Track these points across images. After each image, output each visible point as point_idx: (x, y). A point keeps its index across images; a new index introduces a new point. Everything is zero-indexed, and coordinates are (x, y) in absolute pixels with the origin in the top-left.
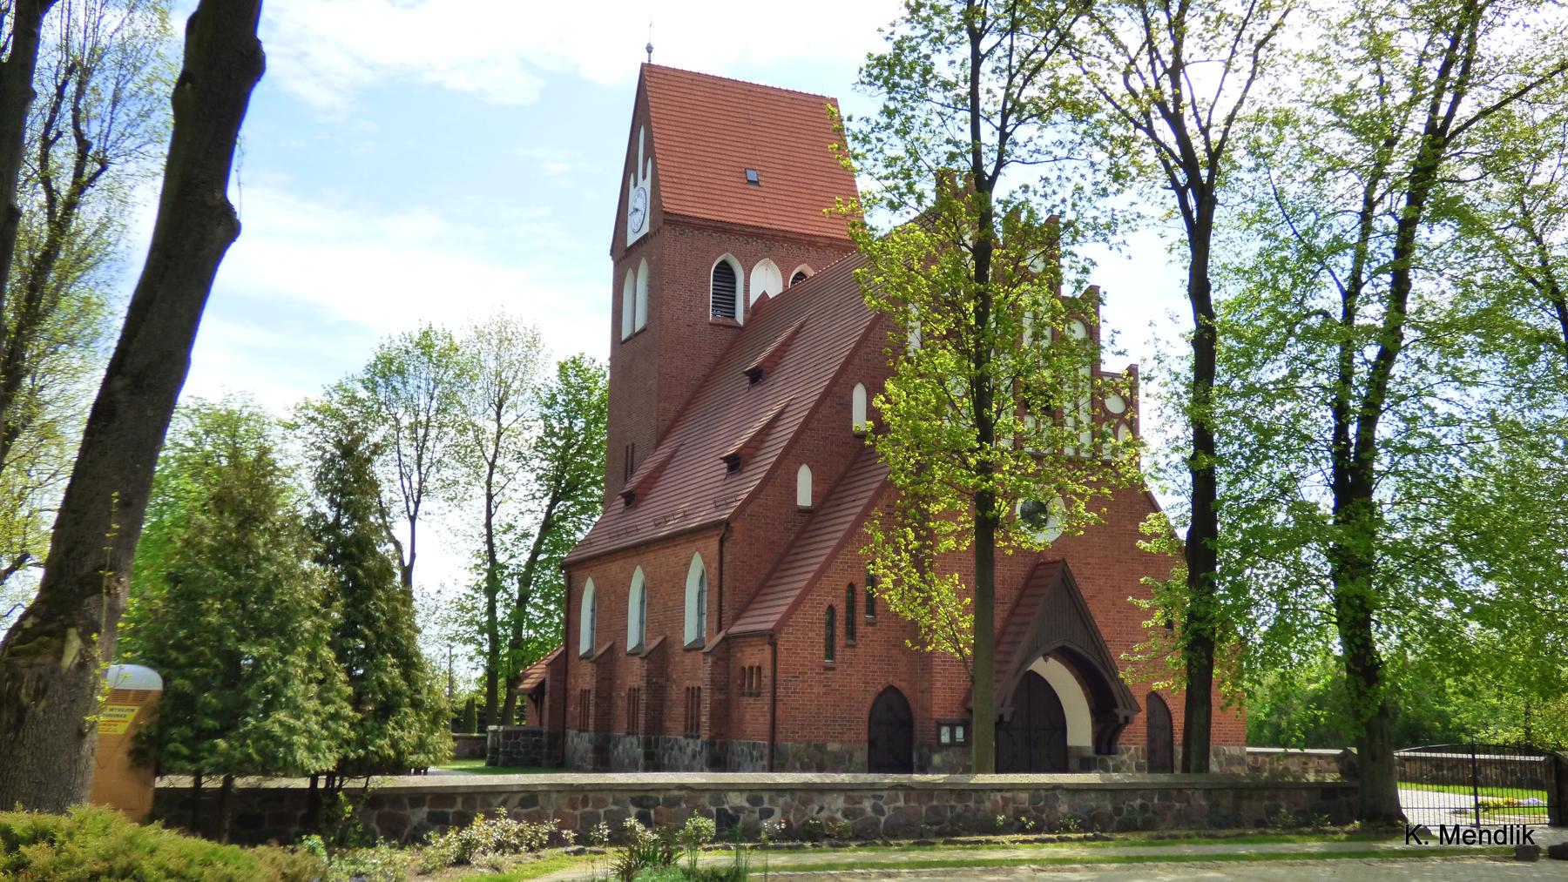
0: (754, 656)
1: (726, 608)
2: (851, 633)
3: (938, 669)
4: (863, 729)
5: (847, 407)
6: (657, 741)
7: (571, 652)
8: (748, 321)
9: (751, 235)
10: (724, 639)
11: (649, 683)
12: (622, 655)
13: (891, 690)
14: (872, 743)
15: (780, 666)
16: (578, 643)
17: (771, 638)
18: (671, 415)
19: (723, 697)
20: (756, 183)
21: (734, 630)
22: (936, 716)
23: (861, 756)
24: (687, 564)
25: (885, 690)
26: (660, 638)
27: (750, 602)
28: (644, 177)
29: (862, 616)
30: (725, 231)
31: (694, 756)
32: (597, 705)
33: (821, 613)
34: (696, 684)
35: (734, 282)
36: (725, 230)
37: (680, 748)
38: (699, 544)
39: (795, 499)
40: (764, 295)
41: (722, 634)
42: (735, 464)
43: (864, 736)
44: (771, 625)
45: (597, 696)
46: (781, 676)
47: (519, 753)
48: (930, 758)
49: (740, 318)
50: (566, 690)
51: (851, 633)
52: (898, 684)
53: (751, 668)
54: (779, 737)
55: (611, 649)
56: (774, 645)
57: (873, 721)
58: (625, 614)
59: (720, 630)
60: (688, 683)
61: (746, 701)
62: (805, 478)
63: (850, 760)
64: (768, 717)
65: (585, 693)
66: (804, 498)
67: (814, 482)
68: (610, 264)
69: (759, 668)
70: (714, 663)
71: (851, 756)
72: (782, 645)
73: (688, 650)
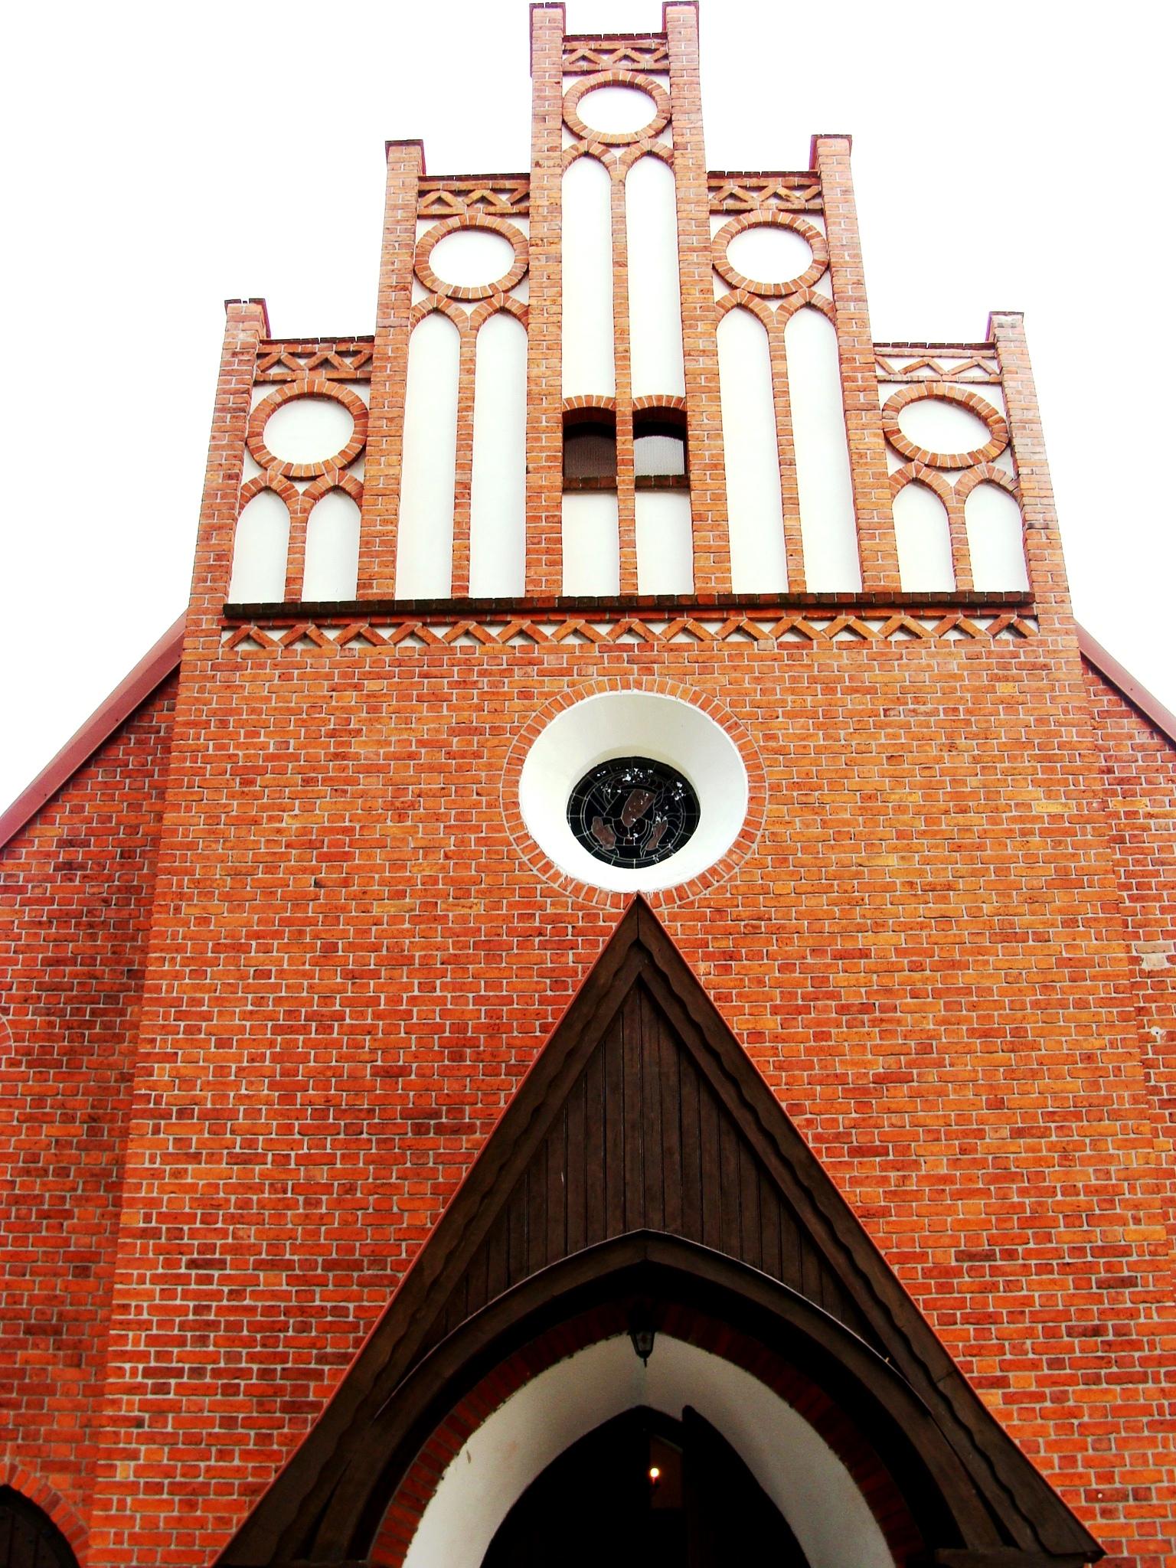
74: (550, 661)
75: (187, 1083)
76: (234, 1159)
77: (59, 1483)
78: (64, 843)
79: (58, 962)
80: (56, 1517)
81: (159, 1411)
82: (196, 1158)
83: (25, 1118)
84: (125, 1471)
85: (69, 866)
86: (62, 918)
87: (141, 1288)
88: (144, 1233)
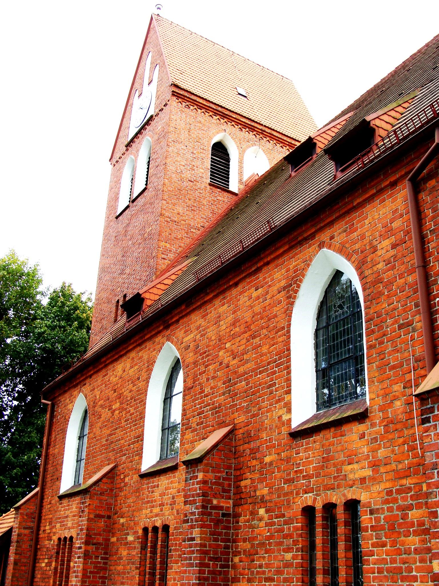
9: (245, 126)
11: (206, 507)
12: (132, 480)
16: (59, 479)
20: (245, 97)
24: (291, 290)
26: (224, 431)
30: (224, 116)
32: (86, 556)
34: (338, 497)
35: (228, 160)
38: (324, 236)
45: (87, 543)
50: (37, 540)
55: (111, 475)
60: (308, 499)
65: (66, 543)
73: (301, 434)
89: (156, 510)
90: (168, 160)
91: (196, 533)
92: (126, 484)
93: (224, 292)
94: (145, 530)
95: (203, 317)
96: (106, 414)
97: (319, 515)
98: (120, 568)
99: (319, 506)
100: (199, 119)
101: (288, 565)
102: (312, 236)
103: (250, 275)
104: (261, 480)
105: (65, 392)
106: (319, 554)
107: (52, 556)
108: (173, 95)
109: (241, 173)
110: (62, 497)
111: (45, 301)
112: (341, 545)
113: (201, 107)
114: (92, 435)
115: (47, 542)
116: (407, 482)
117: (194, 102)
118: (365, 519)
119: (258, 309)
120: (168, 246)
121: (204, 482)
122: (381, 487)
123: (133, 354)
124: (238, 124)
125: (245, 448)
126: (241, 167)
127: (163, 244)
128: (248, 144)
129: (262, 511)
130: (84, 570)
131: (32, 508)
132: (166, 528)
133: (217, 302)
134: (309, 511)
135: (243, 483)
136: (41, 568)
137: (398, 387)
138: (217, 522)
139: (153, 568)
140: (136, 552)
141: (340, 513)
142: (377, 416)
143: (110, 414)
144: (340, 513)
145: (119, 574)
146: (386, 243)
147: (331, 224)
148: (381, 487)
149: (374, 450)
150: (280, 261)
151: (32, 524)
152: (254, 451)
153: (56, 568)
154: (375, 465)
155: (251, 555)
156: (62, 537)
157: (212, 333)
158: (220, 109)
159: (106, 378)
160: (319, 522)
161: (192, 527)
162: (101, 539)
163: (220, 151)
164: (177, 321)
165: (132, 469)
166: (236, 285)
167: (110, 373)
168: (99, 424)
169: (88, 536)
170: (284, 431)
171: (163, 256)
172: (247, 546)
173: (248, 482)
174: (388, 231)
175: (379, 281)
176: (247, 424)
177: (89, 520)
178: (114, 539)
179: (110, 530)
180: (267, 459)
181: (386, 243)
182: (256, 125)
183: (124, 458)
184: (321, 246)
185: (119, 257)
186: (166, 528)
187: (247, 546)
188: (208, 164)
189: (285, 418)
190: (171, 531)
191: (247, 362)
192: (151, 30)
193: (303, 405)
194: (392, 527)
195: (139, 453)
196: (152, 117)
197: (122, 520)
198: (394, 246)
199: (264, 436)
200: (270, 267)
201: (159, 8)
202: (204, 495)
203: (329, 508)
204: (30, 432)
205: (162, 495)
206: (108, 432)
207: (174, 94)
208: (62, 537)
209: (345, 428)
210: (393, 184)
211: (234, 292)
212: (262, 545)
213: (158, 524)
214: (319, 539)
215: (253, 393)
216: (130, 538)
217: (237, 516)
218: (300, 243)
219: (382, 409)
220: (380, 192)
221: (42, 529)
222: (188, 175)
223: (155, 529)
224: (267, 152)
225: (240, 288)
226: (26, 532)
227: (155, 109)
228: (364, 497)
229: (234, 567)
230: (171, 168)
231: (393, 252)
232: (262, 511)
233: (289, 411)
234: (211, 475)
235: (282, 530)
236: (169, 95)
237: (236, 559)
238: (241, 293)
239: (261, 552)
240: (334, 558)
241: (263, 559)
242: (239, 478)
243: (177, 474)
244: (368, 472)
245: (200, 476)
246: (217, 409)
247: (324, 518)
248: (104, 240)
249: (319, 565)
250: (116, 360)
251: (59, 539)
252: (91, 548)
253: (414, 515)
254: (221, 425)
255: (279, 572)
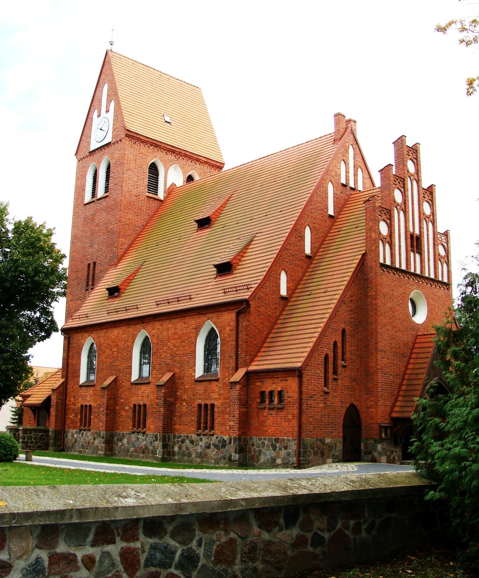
0: (269, 386)
1: (242, 354)
2: (335, 372)
3: (380, 394)
4: (341, 429)
5: (303, 238)
6: (169, 437)
7: (71, 383)
8: (166, 198)
10: (247, 374)
11: (165, 401)
12: (126, 385)
13: (352, 406)
14: (344, 438)
15: (304, 390)
16: (78, 376)
17: (297, 373)
18: (125, 246)
19: (245, 410)
21: (252, 368)
22: (379, 421)
23: (340, 447)
24: (197, 330)
25: (350, 406)
27: (259, 351)
28: (107, 111)
29: (340, 362)
31: (208, 447)
33: (322, 359)
34: (209, 402)
35: (157, 175)
36: (156, 145)
37: (192, 442)
38: (210, 315)
39: (279, 290)
40: (173, 185)
41: (241, 373)
42: (224, 269)
43: (341, 434)
44: (299, 365)
45: (107, 409)
46: (304, 396)
47: (32, 442)
48: (377, 446)
49: (161, 195)
50: (66, 405)
51: (335, 372)
52: (355, 403)
53: (271, 392)
54: (303, 434)
55: (115, 381)
56: (300, 377)
57: (345, 426)
58: (131, 358)
59: (237, 369)
60: (200, 401)
61: (265, 413)
62: (283, 278)
63: (335, 448)
64: (295, 423)
66: (283, 292)
67: (288, 282)
68: (75, 161)
69: (280, 393)
70: (241, 388)
71: (336, 445)
72: (305, 379)
73: (198, 381)
74: (411, 283)
75: (382, 346)
76: (387, 359)
77: (358, 403)
78: (351, 296)
79: (351, 318)
80: (358, 408)
81: (382, 395)
82: (384, 358)
83: (350, 345)
84: (380, 403)
85: (351, 301)
86: (351, 310)
87: (380, 378)
88: (380, 369)
89: (140, 398)
90: (124, 184)
91: (162, 409)
92: (123, 386)
93: (171, 319)
94: (135, 405)
95: (161, 325)
96: (108, 352)
97: (203, 407)
98: (122, 419)
99: (203, 404)
100: (142, 151)
101: (192, 421)
102: (206, 314)
103: (182, 317)
104: (184, 394)
105: (78, 333)
106: (202, 418)
107: (77, 413)
108: (126, 136)
109: (165, 186)
110: (81, 386)
111: (10, 227)
112: (209, 416)
113: (143, 142)
114: (100, 360)
115: (72, 406)
116: (227, 401)
117: (139, 139)
118: (216, 409)
119: (184, 332)
120: (124, 240)
121: (165, 393)
122: (221, 401)
123: (124, 328)
124: (164, 150)
125: (179, 382)
126: (166, 181)
127: (121, 239)
128: (170, 163)
129: (184, 404)
130: (106, 421)
131: (61, 390)
132: (145, 406)
133: (167, 322)
134: (200, 405)
135: (178, 393)
136: (70, 418)
137: (227, 374)
138: (169, 406)
139: (139, 419)
140: (130, 414)
141: (209, 407)
142: (221, 381)
143: (111, 352)
144: (209, 407)
145: (121, 422)
146: (228, 328)
147: (212, 313)
148: (221, 401)
149: (220, 391)
150: (194, 317)
151: (62, 397)
152: (182, 383)
153: (81, 419)
154: (219, 395)
155: (180, 417)
156: (84, 405)
157: (165, 333)
158: (154, 142)
159: (107, 334)
160: (203, 409)
161: (160, 407)
162: (112, 408)
163: (153, 168)
164: (148, 322)
165: (126, 380)
166: (176, 318)
167: (110, 332)
168: (105, 355)
169: (107, 407)
170: (193, 378)
171: (121, 247)
172: (179, 414)
173: (179, 393)
174: (229, 325)
175: (225, 340)
176: (180, 373)
177: (107, 400)
178: (118, 408)
179: (116, 404)
180: (187, 387)
181: (228, 328)
182: (176, 149)
183: (121, 374)
184: (208, 319)
185: (89, 234)
186: (145, 406)
187: (179, 414)
188: (146, 183)
189: (193, 374)
190: (147, 406)
191: (180, 350)
192: (106, 63)
193: (199, 371)
194: (223, 413)
195: (130, 374)
196: (110, 143)
197: (122, 400)
198: (230, 330)
199: (186, 379)
200: (190, 317)
201: (111, 44)
202: (165, 397)
203: (206, 405)
204: (13, 328)
205: (143, 393)
206: (111, 361)
207: (127, 135)
208: (84, 405)
209: (212, 382)
210: (232, 310)
211: (175, 321)
212: (184, 414)
213: (141, 403)
214: (202, 414)
215: (182, 363)
216: (127, 408)
217: (175, 404)
218: (201, 314)
219: (223, 379)
220: (229, 310)
221: (68, 400)
222: (135, 192)
223: (140, 406)
224: (182, 167)
225: (177, 320)
226: (60, 401)
227: (113, 137)
228: (216, 403)
229: (174, 420)
230: (125, 189)
231: (229, 332)
232: (184, 404)
233: (195, 372)
234: (167, 390)
235: (191, 410)
236: (123, 136)
237: (175, 418)
238: (178, 323)
239: (184, 416)
240: (207, 419)
241: (184, 419)
242: (176, 391)
243: (149, 385)
244: (217, 397)
245: (163, 391)
246: (167, 365)
247: (204, 408)
248: (74, 215)
249: (202, 421)
250: (114, 327)
251: (82, 406)
252: (108, 411)
253: (228, 410)
254: (169, 371)
255: (189, 423)
